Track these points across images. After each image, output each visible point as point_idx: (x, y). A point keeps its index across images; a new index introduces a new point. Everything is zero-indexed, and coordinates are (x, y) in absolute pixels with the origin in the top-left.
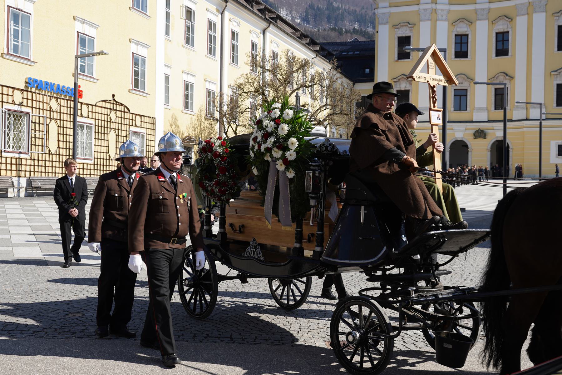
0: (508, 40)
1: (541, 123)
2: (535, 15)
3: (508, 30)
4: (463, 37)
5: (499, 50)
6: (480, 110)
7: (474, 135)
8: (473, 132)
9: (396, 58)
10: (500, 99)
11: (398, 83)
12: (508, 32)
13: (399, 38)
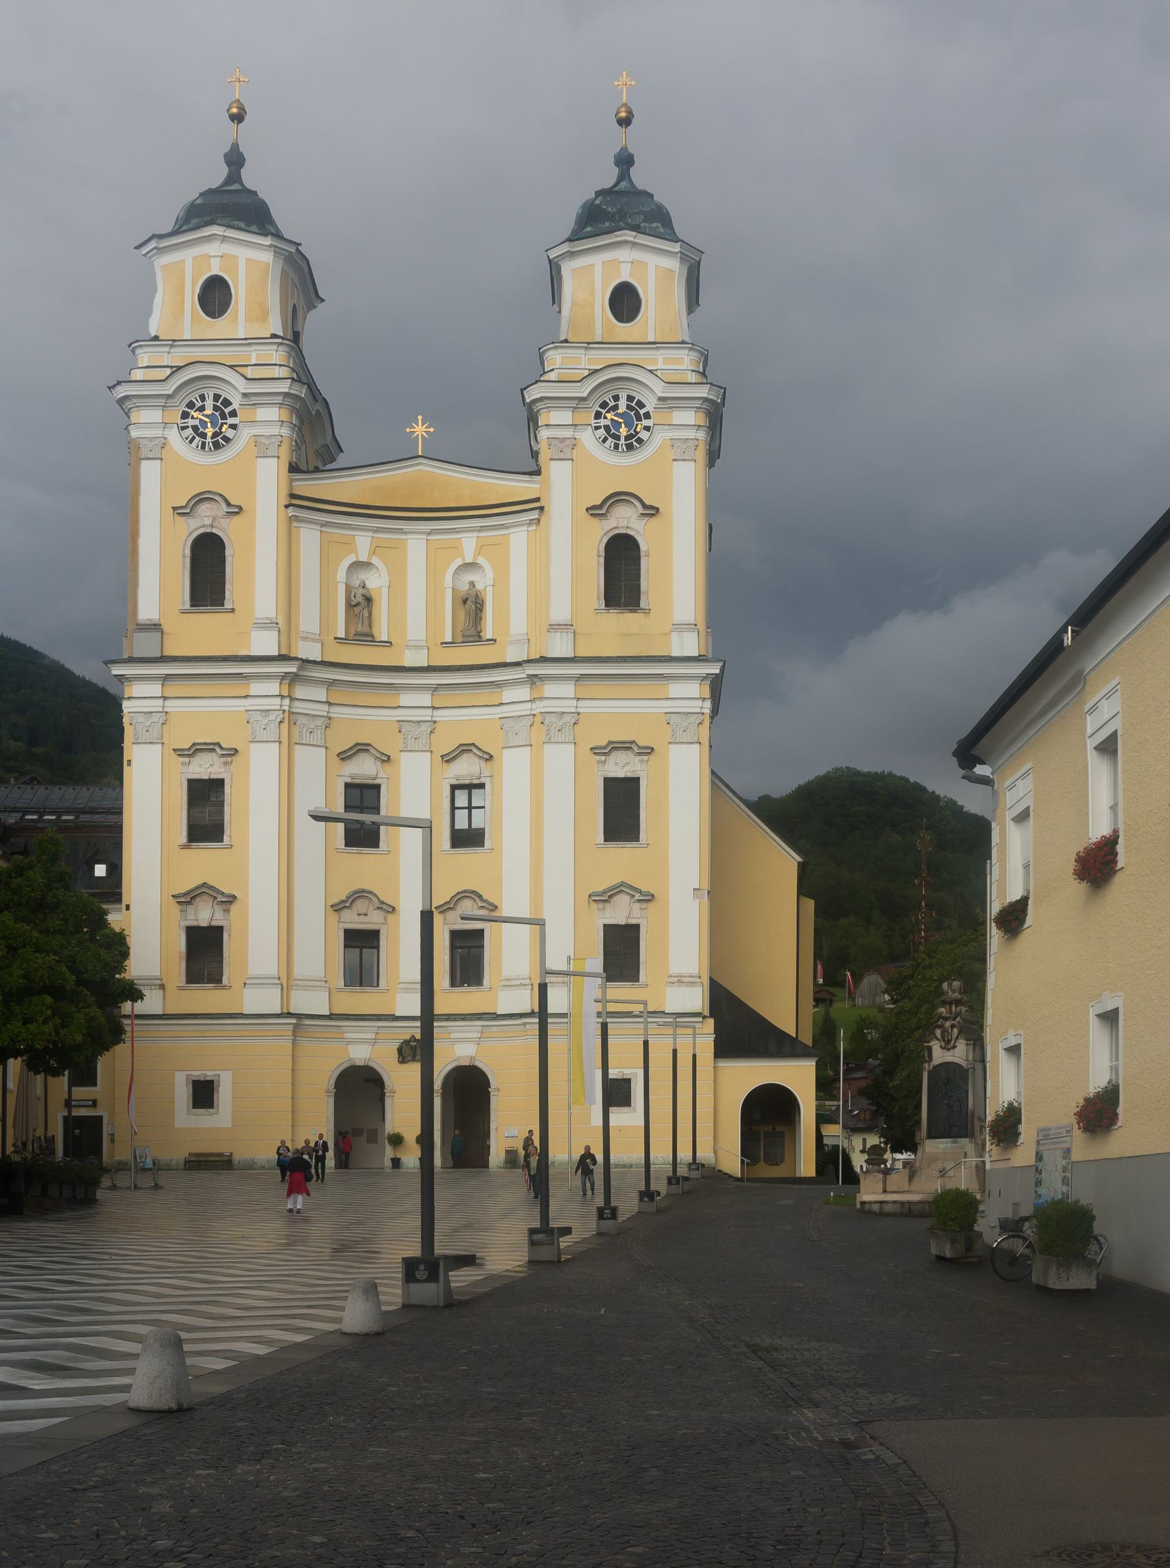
3: (482, 780)
7: (400, 1050)
8: (397, 1045)
9: (183, 838)
11: (190, 908)
13: (191, 782)
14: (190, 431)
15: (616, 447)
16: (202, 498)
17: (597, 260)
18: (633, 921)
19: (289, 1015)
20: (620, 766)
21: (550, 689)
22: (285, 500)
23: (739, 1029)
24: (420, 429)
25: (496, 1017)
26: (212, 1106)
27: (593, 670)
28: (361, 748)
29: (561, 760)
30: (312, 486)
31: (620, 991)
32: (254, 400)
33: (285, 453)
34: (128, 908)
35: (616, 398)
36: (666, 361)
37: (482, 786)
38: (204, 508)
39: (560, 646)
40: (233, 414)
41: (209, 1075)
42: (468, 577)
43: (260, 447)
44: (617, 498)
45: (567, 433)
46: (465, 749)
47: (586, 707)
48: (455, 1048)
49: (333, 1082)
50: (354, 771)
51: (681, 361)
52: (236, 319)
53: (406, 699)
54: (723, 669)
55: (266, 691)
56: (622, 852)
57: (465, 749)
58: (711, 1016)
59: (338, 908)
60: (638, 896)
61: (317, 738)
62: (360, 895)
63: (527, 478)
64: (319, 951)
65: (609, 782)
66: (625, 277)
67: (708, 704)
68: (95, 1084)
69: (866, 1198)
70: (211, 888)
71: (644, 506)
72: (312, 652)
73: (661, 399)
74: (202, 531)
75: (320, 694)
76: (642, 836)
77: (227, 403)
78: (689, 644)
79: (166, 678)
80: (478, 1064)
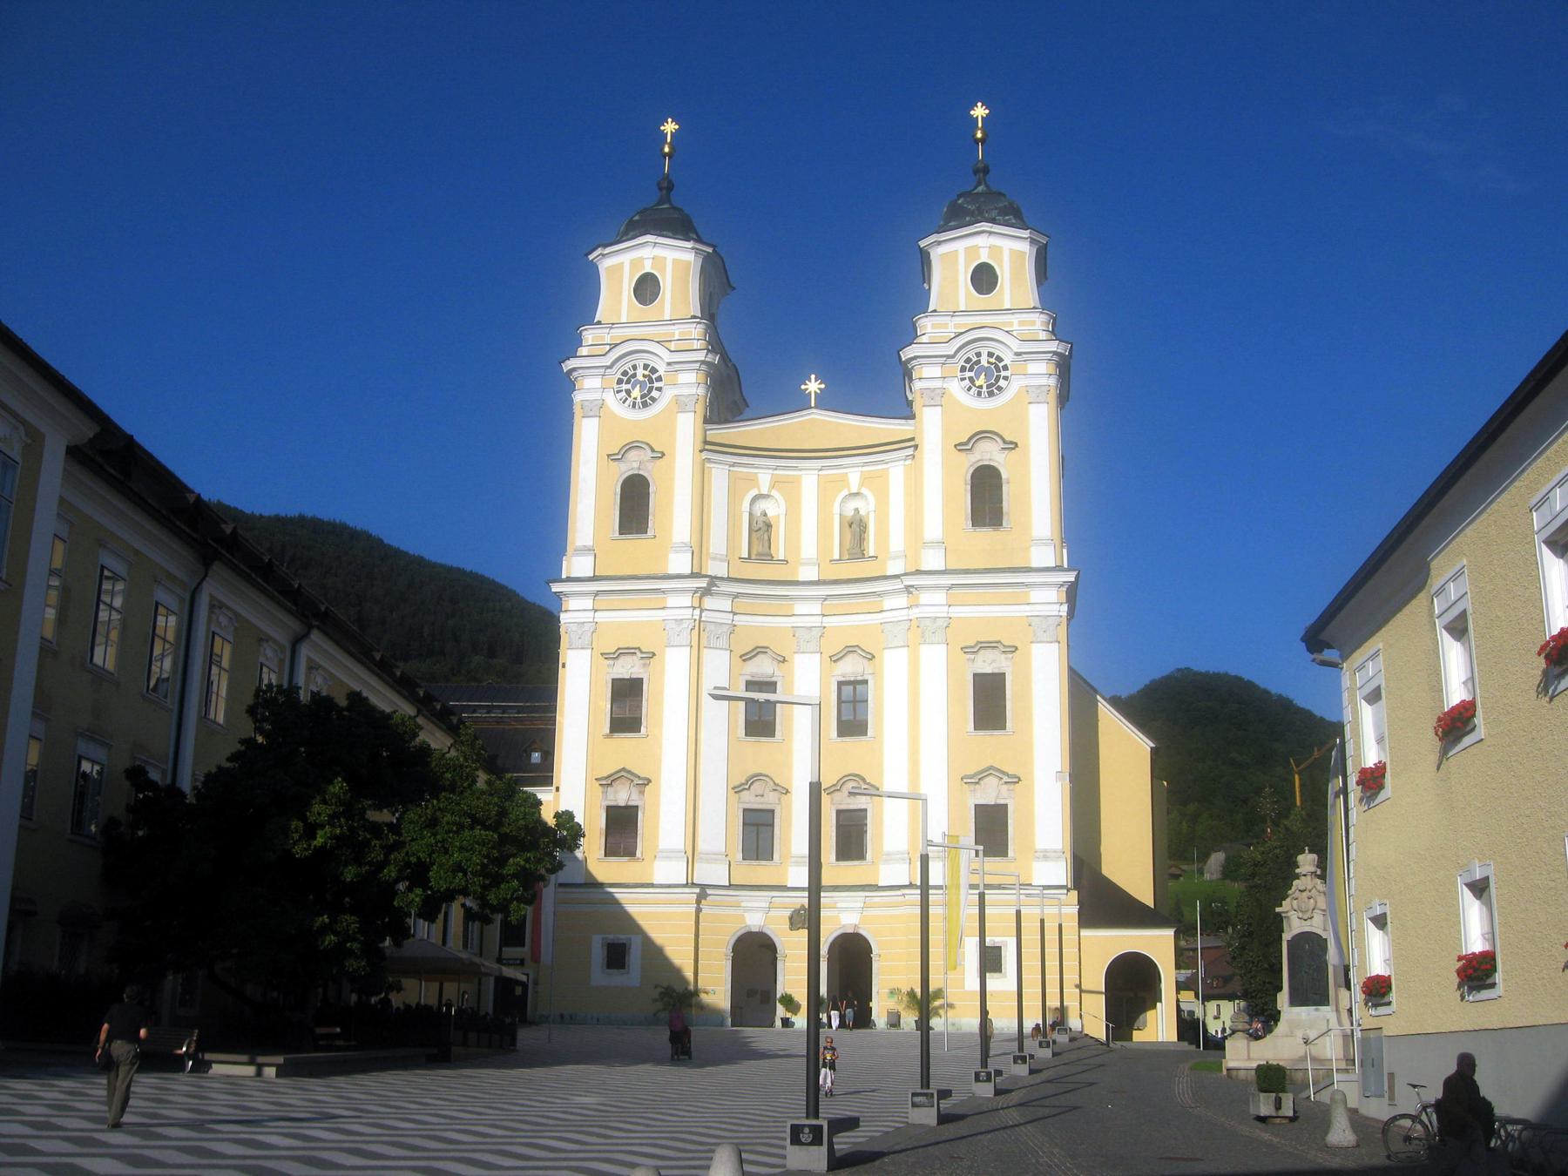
1: (982, 896)
2: (924, 649)
5: (848, 722)
7: (791, 918)
8: (788, 913)
12: (866, 682)
15: (979, 394)
16: (632, 447)
19: (694, 885)
20: (987, 663)
21: (925, 597)
22: (700, 446)
23: (1102, 903)
24: (813, 386)
25: (876, 888)
28: (759, 651)
29: (935, 658)
30: (721, 433)
31: (993, 864)
32: (677, 367)
33: (700, 408)
35: (978, 354)
36: (1021, 323)
37: (866, 682)
38: (632, 455)
42: (853, 504)
43: (680, 404)
44: (981, 435)
45: (938, 384)
46: (850, 650)
47: (956, 612)
48: (840, 916)
50: (755, 670)
51: (1033, 323)
52: (662, 306)
53: (799, 608)
54: (1077, 577)
55: (680, 603)
56: (990, 738)
57: (850, 650)
59: (738, 789)
60: (1006, 779)
61: (723, 642)
62: (756, 778)
64: (719, 829)
66: (984, 258)
67: (1065, 608)
69: (1231, 1064)
70: (629, 772)
71: (1005, 442)
72: (716, 568)
73: (1018, 354)
75: (726, 604)
76: (1008, 724)
77: (654, 370)
78: (1045, 555)
79: (597, 593)
80: (862, 932)
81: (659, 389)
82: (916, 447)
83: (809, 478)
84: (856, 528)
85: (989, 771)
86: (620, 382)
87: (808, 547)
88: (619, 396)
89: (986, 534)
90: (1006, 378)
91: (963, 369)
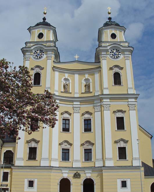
0: (91, 124)
4: (67, 121)
6: (77, 161)
10: (88, 154)
14: (35, 56)
17: (108, 30)
18: (124, 146)
20: (120, 115)
26: (33, 187)
27: (113, 97)
34: (17, 143)
39: (106, 92)
40: (43, 53)
41: (32, 180)
49: (59, 182)
58: (142, 167)
63: (97, 63)
64: (57, 153)
65: (118, 118)
68: (8, 181)
72: (57, 94)
74: (36, 72)
77: (42, 51)
81: (43, 55)
82: (101, 68)
83: (77, 76)
84: (87, 86)
85: (122, 140)
86: (34, 53)
87: (77, 90)
88: (34, 56)
89: (117, 87)
90: (120, 55)
91: (111, 52)
